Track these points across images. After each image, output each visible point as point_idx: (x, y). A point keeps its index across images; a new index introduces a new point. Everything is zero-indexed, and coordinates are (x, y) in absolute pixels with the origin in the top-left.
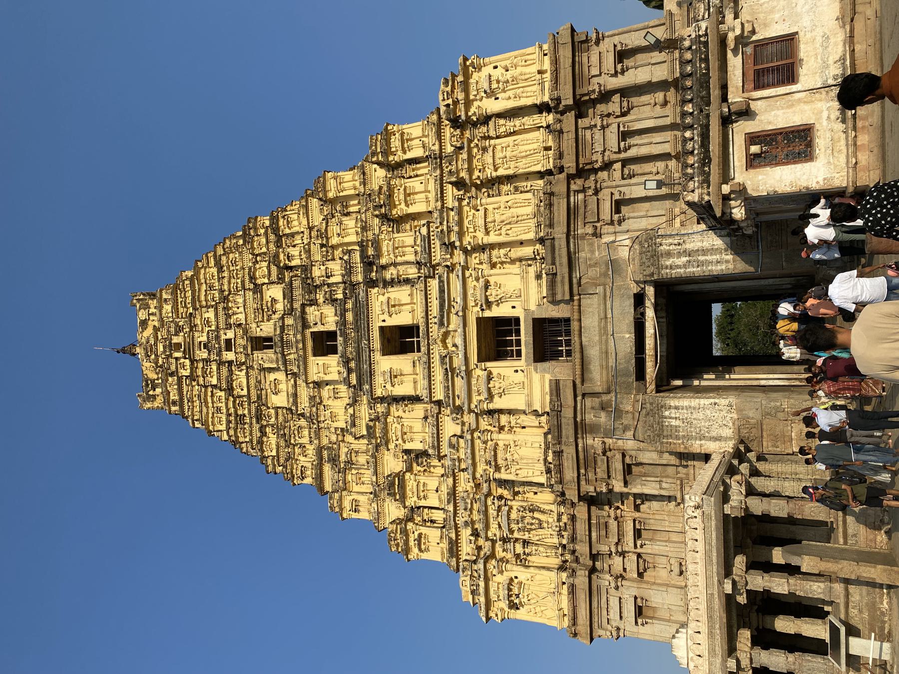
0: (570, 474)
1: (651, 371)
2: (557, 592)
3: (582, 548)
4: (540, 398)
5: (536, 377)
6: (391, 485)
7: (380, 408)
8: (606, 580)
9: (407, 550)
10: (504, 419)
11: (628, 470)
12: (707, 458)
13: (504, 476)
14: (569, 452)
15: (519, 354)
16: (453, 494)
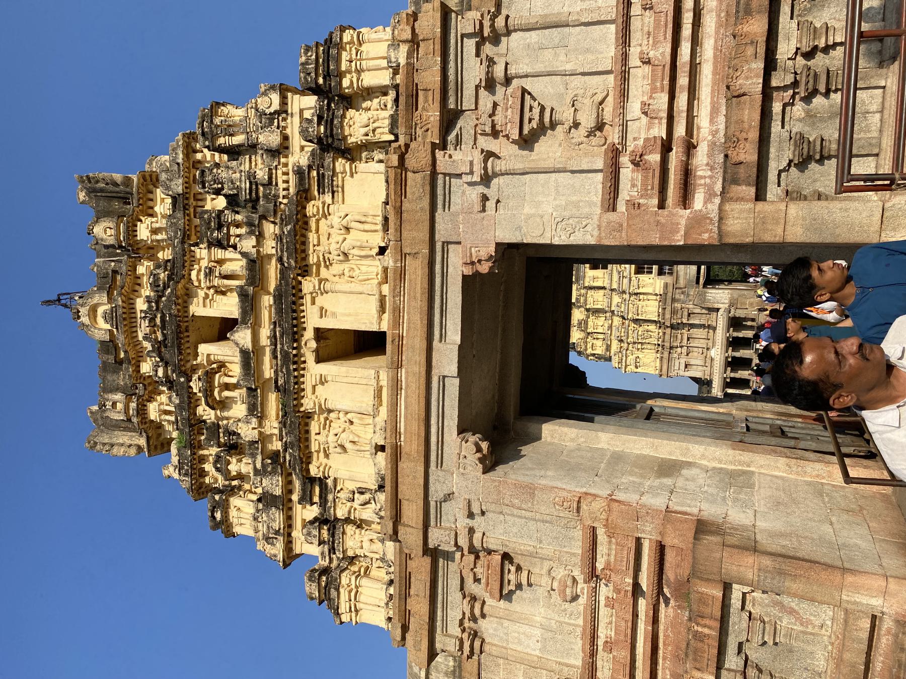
0: (668, 316)
1: (702, 281)
2: (655, 361)
3: (667, 345)
4: (659, 289)
5: (658, 281)
6: (580, 323)
7: (583, 291)
8: (675, 355)
9: (586, 350)
10: (641, 297)
11: (689, 315)
12: (718, 310)
13: (640, 317)
14: (668, 309)
15: (651, 273)
16: (610, 327)
